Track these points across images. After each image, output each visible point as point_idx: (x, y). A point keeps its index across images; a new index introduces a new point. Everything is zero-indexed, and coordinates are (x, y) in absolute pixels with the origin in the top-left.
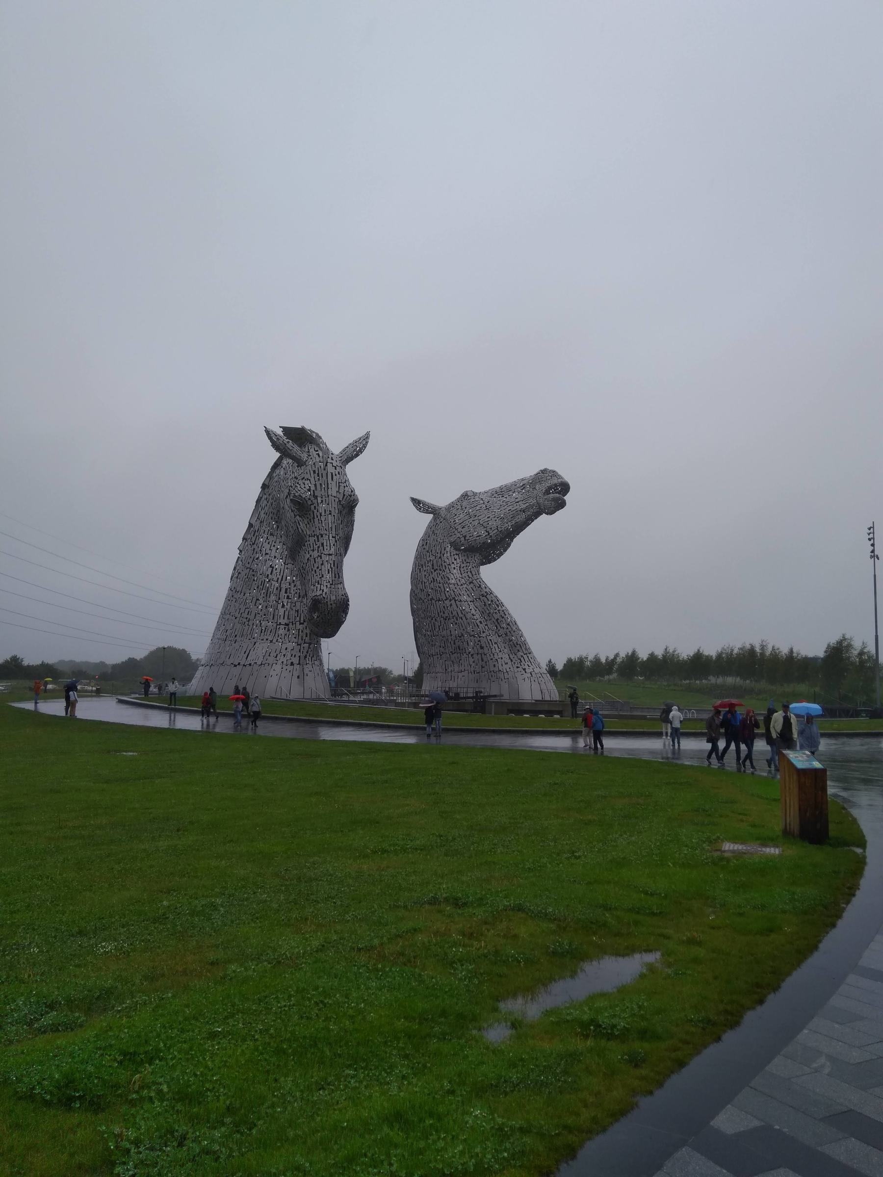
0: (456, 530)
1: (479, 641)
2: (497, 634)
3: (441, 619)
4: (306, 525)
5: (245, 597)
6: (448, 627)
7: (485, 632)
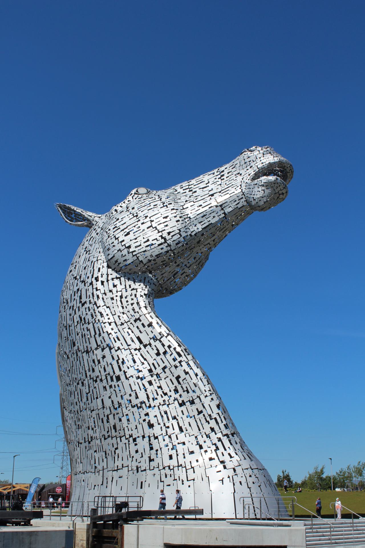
0: (116, 239)
1: (147, 414)
2: (176, 402)
3: (90, 381)
6: (98, 394)
7: (156, 399)
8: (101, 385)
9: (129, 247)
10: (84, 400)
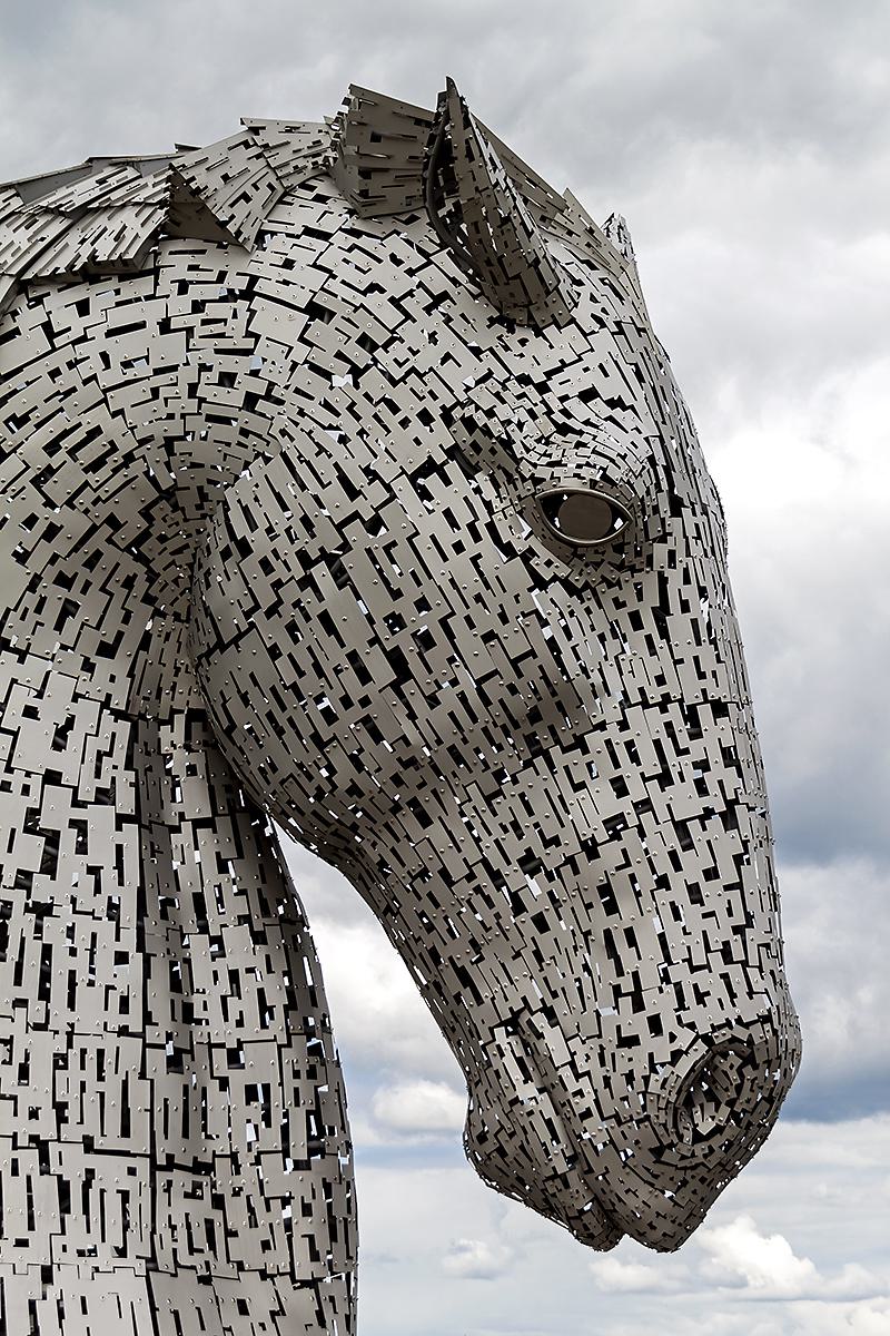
4: (602, 638)
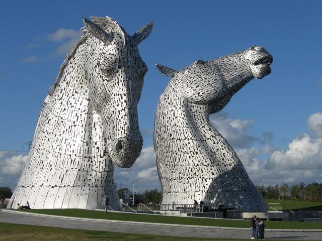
5: (56, 138)
8: (188, 156)
9: (199, 94)
10: (178, 160)
